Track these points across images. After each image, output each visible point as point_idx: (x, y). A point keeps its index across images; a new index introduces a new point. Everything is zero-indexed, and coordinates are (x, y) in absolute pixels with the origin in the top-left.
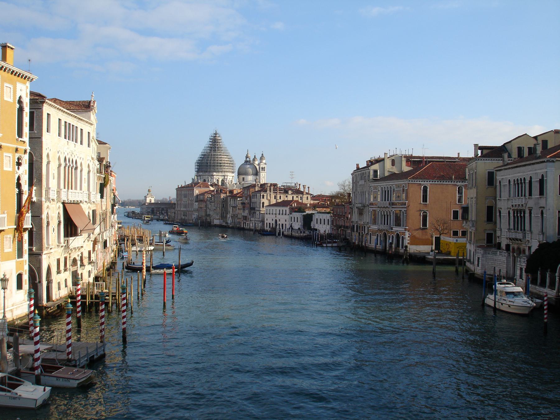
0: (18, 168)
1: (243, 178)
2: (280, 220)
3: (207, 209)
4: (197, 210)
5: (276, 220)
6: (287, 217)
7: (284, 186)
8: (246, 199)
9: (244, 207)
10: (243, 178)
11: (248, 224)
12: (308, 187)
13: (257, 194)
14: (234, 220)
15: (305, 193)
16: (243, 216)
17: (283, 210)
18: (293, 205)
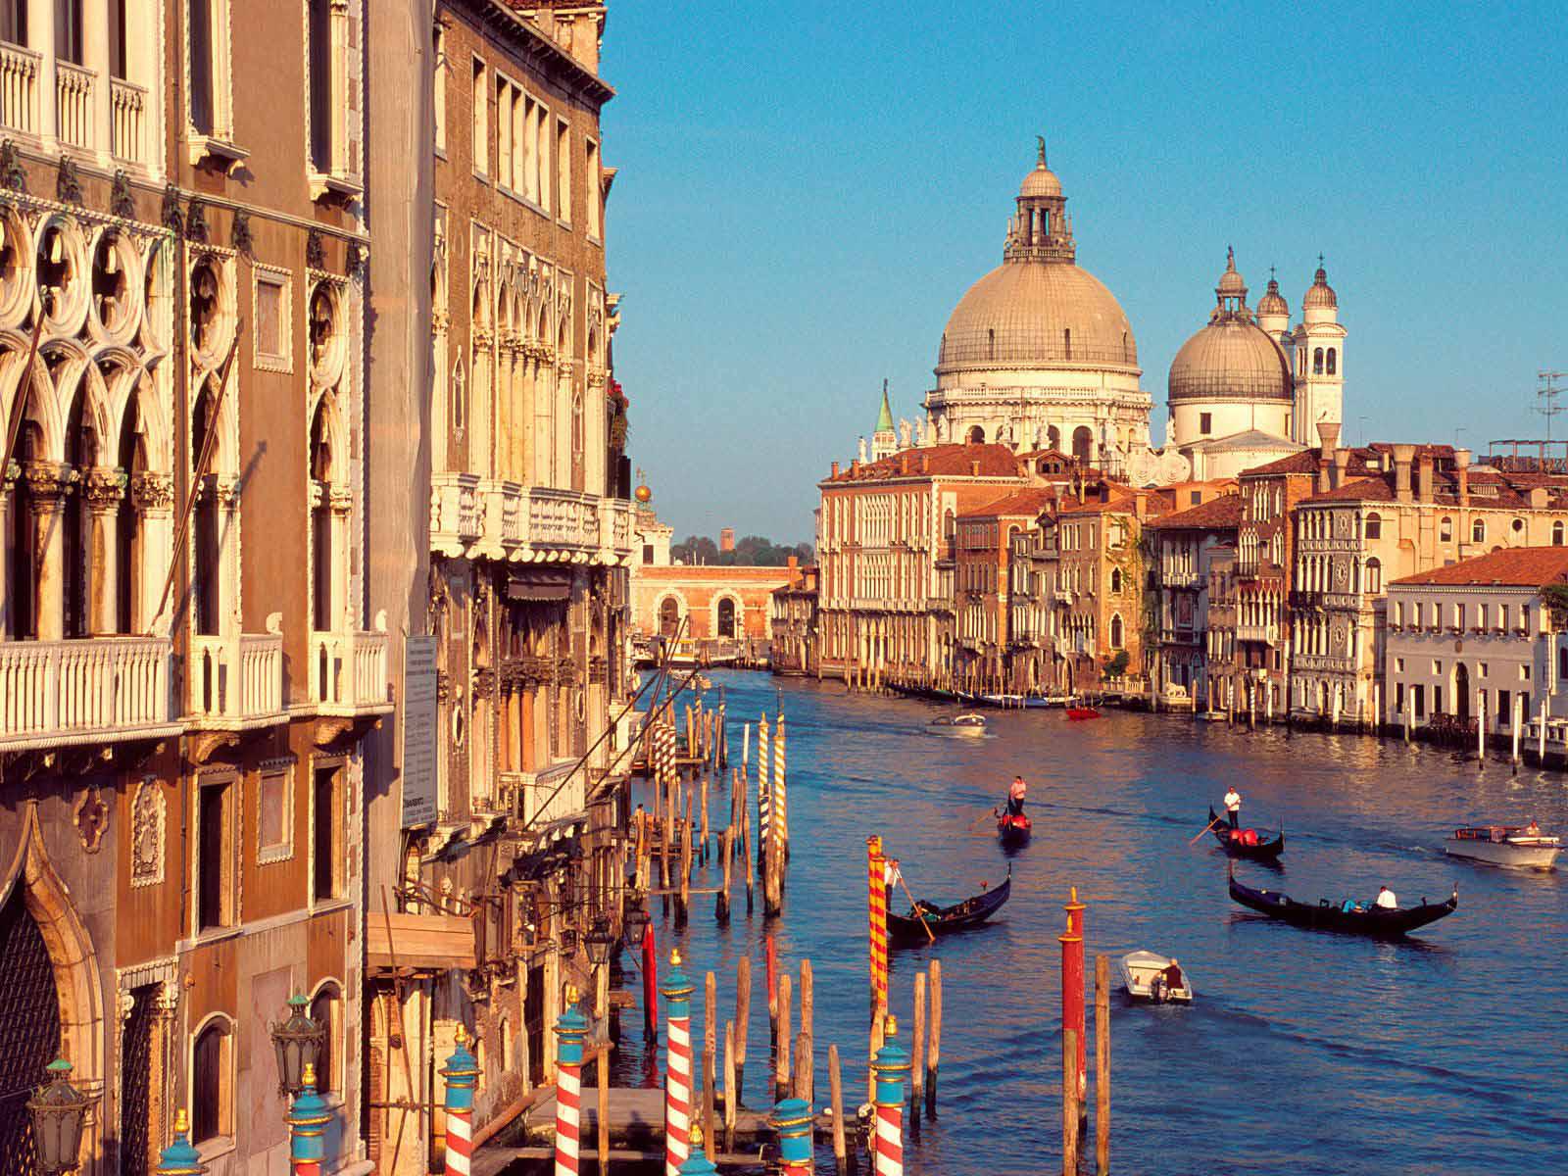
0: (315, 358)
1: (1206, 419)
7: (1496, 462)
8: (1263, 544)
10: (1206, 419)
11: (1276, 688)
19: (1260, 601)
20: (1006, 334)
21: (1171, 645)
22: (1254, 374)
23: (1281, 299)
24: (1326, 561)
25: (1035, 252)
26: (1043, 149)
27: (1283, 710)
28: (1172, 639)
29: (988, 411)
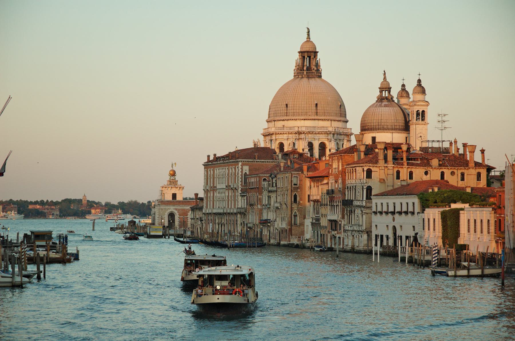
1: (374, 139)
2: (401, 226)
3: (261, 210)
4: (243, 213)
5: (394, 228)
6: (415, 220)
7: (422, 149)
9: (332, 200)
10: (374, 139)
12: (483, 151)
13: (357, 168)
14: (317, 232)
15: (472, 164)
16: (330, 221)
17: (407, 204)
18: (430, 190)
19: (335, 204)
20: (293, 106)
21: (314, 223)
22: (393, 121)
23: (407, 93)
24: (354, 188)
25: (305, 73)
26: (309, 32)
27: (341, 247)
28: (314, 221)
29: (285, 136)
